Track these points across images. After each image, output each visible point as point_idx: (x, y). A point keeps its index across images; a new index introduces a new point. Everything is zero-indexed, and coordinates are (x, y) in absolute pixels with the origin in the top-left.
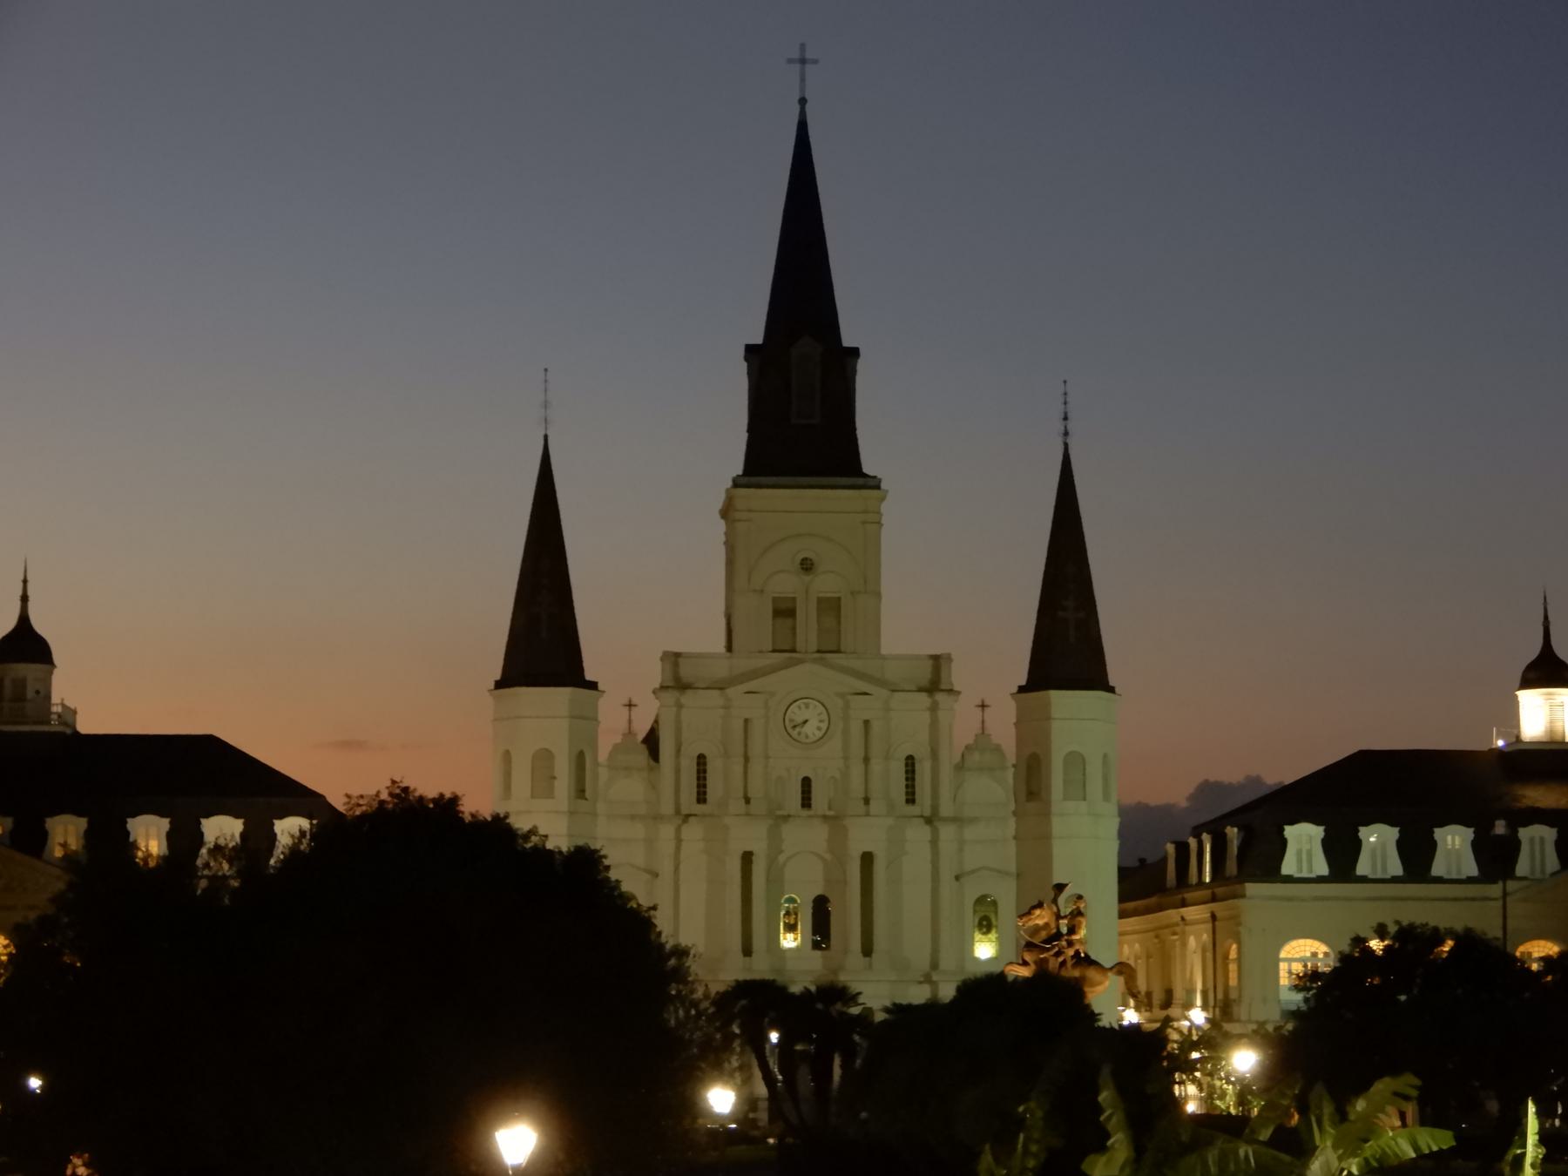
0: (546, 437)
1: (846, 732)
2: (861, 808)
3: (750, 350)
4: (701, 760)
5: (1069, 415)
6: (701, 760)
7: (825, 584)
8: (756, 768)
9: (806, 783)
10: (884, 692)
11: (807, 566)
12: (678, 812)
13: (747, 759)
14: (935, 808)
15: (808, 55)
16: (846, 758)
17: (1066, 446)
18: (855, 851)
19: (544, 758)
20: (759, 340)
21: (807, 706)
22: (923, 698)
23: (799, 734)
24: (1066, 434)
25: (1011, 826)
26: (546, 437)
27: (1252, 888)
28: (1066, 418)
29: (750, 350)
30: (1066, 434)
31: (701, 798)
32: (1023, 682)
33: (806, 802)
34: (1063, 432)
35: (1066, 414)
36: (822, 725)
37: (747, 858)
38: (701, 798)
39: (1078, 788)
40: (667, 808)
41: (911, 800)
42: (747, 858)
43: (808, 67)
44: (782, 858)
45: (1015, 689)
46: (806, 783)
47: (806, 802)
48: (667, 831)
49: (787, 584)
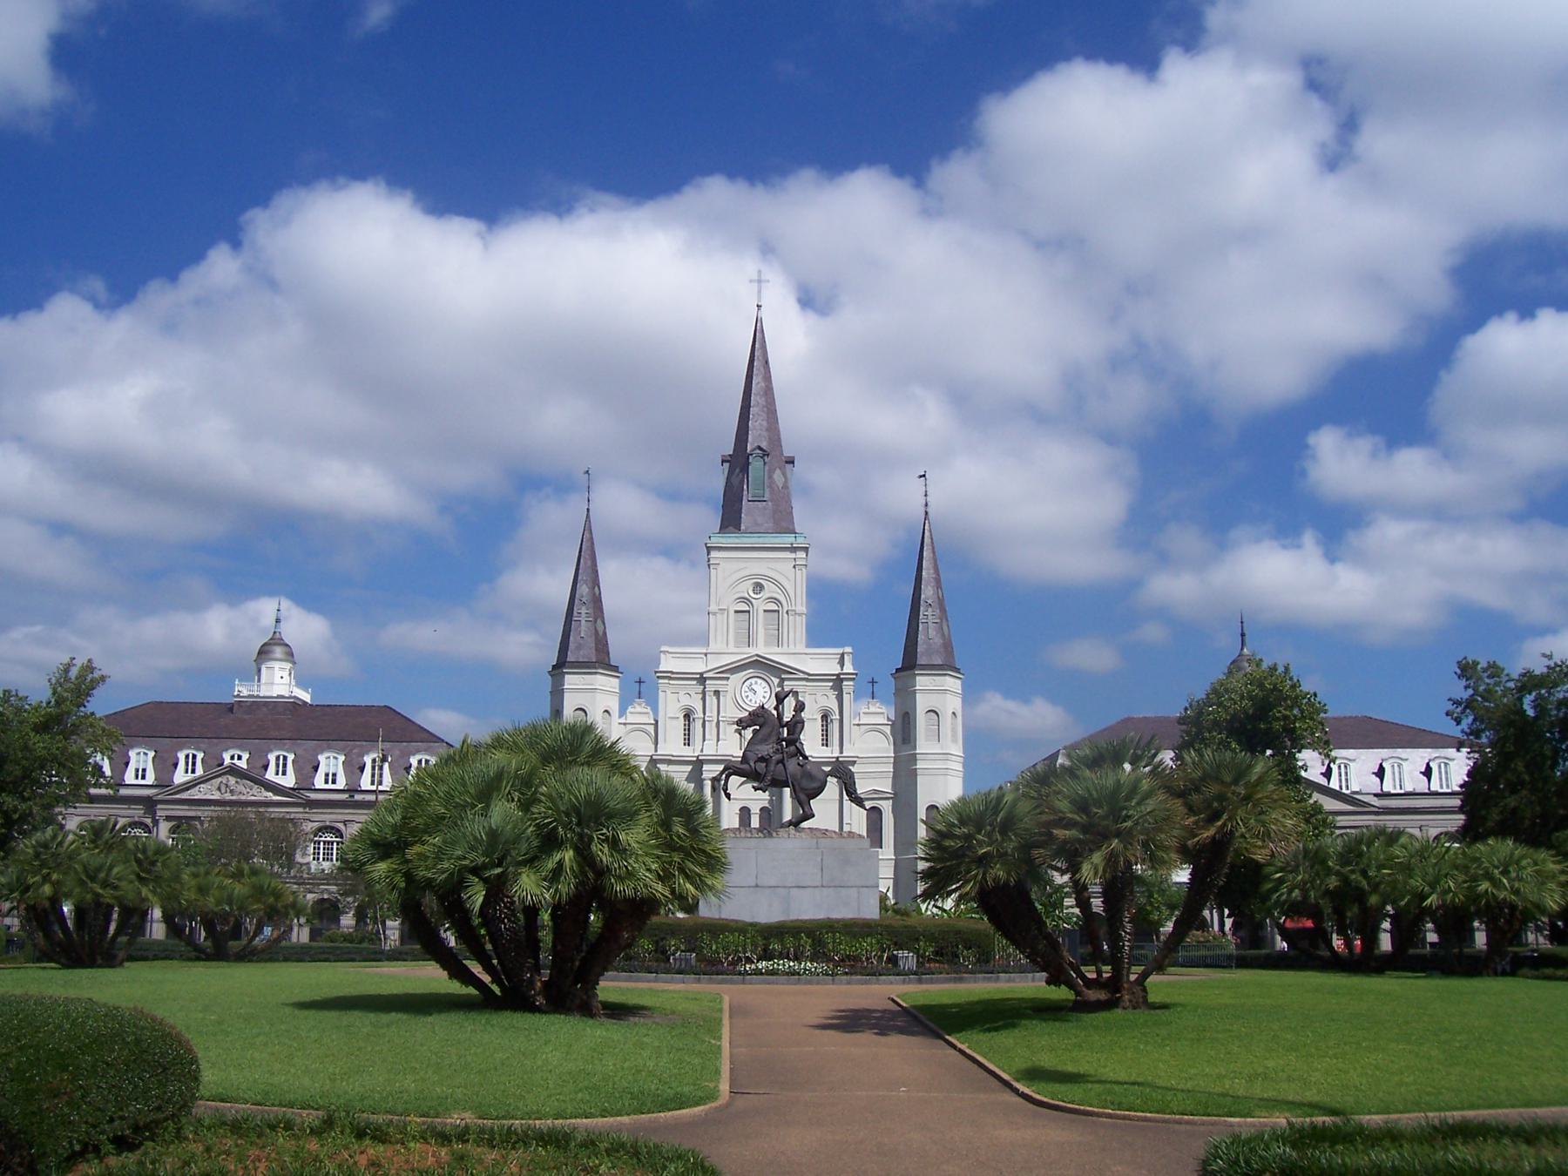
0: (588, 510)
5: (928, 493)
15: (763, 278)
20: (731, 453)
21: (756, 683)
23: (751, 700)
24: (926, 505)
26: (588, 510)
28: (926, 495)
30: (926, 505)
32: (900, 666)
34: (924, 503)
35: (926, 491)
36: (765, 695)
43: (763, 285)
45: (894, 671)
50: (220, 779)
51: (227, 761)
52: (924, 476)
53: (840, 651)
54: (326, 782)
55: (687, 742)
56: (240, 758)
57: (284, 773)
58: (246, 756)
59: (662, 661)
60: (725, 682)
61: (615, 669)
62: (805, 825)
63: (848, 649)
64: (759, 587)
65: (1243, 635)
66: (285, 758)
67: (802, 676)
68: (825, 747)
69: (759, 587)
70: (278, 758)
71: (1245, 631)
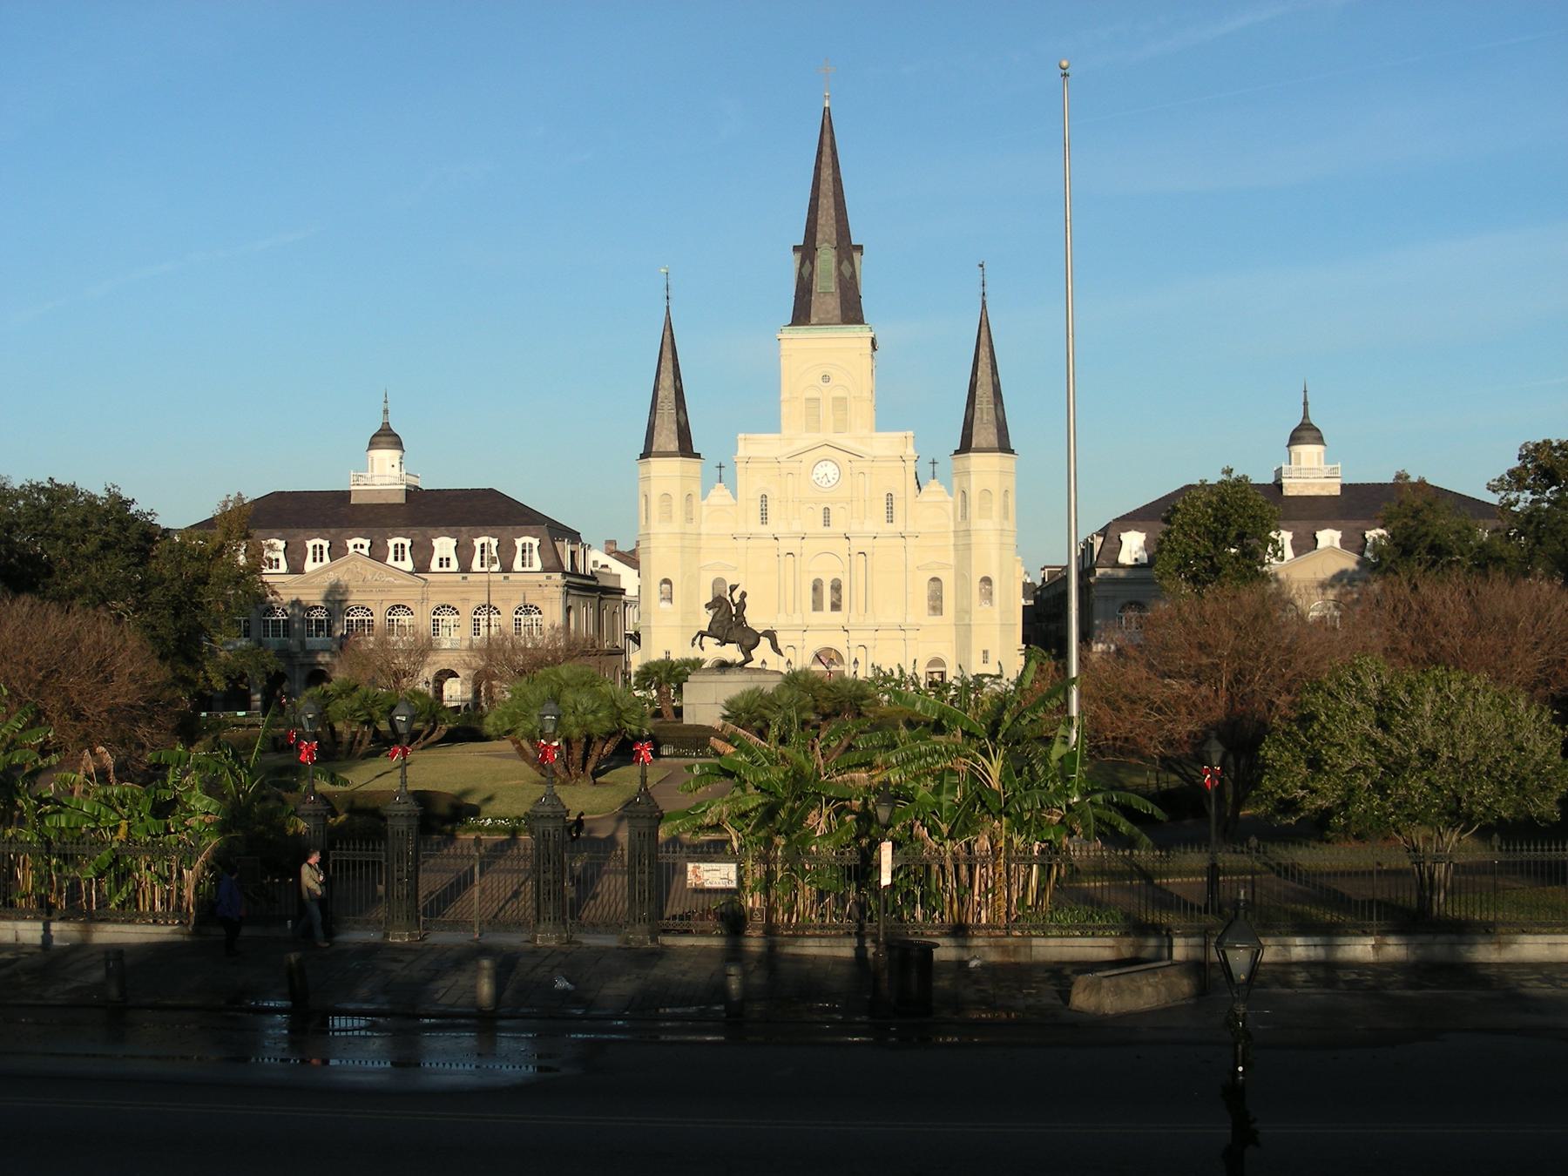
0: (668, 308)
17: (984, 303)
26: (668, 308)
29: (796, 248)
50: (345, 568)
51: (351, 550)
52: (981, 266)
53: (904, 434)
54: (441, 565)
55: (764, 519)
56: (362, 546)
57: (403, 559)
58: (367, 543)
59: (741, 444)
60: (797, 465)
61: (698, 456)
62: (747, 665)
63: (910, 433)
64: (826, 378)
65: (1306, 404)
66: (403, 546)
67: (867, 458)
68: (890, 524)
69: (826, 378)
70: (396, 546)
71: (1308, 400)
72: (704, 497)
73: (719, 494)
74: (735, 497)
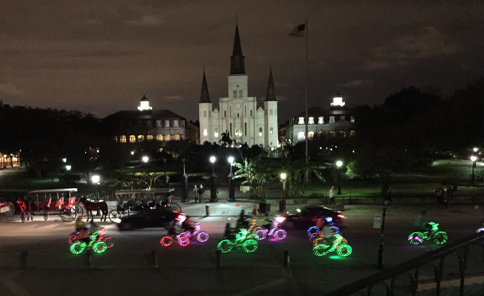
1: (243, 107)
2: (245, 117)
3: (231, 57)
4: (225, 112)
6: (225, 112)
7: (240, 88)
8: (232, 112)
9: (238, 114)
10: (247, 102)
11: (238, 86)
12: (222, 118)
13: (231, 111)
14: (254, 117)
16: (243, 110)
18: (229, 122)
19: (205, 112)
22: (252, 103)
25: (264, 119)
27: (295, 126)
29: (231, 57)
31: (225, 116)
33: (238, 116)
37: (231, 124)
38: (225, 116)
39: (272, 114)
40: (221, 117)
41: (251, 115)
42: (231, 124)
44: (235, 123)
46: (238, 114)
47: (238, 116)
48: (221, 121)
49: (235, 89)
72: (213, 111)
73: (216, 110)
74: (219, 111)
